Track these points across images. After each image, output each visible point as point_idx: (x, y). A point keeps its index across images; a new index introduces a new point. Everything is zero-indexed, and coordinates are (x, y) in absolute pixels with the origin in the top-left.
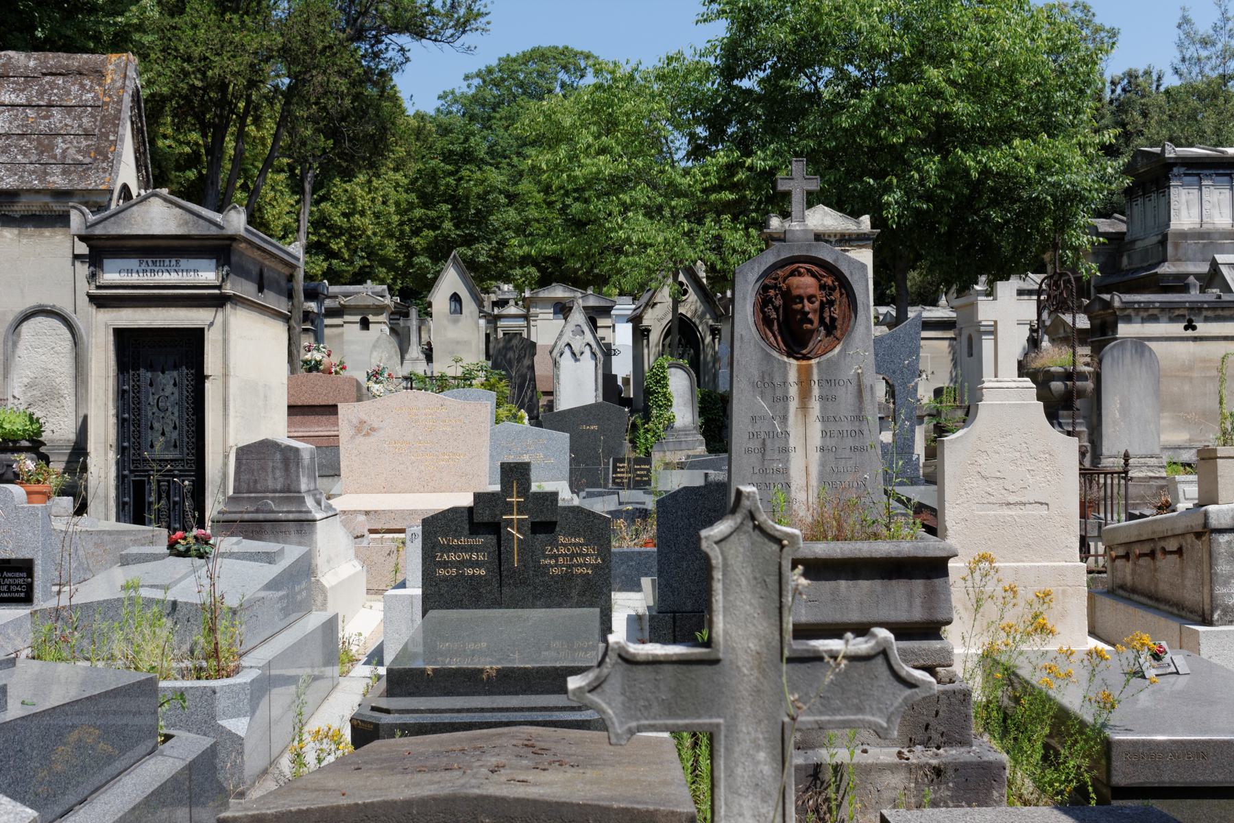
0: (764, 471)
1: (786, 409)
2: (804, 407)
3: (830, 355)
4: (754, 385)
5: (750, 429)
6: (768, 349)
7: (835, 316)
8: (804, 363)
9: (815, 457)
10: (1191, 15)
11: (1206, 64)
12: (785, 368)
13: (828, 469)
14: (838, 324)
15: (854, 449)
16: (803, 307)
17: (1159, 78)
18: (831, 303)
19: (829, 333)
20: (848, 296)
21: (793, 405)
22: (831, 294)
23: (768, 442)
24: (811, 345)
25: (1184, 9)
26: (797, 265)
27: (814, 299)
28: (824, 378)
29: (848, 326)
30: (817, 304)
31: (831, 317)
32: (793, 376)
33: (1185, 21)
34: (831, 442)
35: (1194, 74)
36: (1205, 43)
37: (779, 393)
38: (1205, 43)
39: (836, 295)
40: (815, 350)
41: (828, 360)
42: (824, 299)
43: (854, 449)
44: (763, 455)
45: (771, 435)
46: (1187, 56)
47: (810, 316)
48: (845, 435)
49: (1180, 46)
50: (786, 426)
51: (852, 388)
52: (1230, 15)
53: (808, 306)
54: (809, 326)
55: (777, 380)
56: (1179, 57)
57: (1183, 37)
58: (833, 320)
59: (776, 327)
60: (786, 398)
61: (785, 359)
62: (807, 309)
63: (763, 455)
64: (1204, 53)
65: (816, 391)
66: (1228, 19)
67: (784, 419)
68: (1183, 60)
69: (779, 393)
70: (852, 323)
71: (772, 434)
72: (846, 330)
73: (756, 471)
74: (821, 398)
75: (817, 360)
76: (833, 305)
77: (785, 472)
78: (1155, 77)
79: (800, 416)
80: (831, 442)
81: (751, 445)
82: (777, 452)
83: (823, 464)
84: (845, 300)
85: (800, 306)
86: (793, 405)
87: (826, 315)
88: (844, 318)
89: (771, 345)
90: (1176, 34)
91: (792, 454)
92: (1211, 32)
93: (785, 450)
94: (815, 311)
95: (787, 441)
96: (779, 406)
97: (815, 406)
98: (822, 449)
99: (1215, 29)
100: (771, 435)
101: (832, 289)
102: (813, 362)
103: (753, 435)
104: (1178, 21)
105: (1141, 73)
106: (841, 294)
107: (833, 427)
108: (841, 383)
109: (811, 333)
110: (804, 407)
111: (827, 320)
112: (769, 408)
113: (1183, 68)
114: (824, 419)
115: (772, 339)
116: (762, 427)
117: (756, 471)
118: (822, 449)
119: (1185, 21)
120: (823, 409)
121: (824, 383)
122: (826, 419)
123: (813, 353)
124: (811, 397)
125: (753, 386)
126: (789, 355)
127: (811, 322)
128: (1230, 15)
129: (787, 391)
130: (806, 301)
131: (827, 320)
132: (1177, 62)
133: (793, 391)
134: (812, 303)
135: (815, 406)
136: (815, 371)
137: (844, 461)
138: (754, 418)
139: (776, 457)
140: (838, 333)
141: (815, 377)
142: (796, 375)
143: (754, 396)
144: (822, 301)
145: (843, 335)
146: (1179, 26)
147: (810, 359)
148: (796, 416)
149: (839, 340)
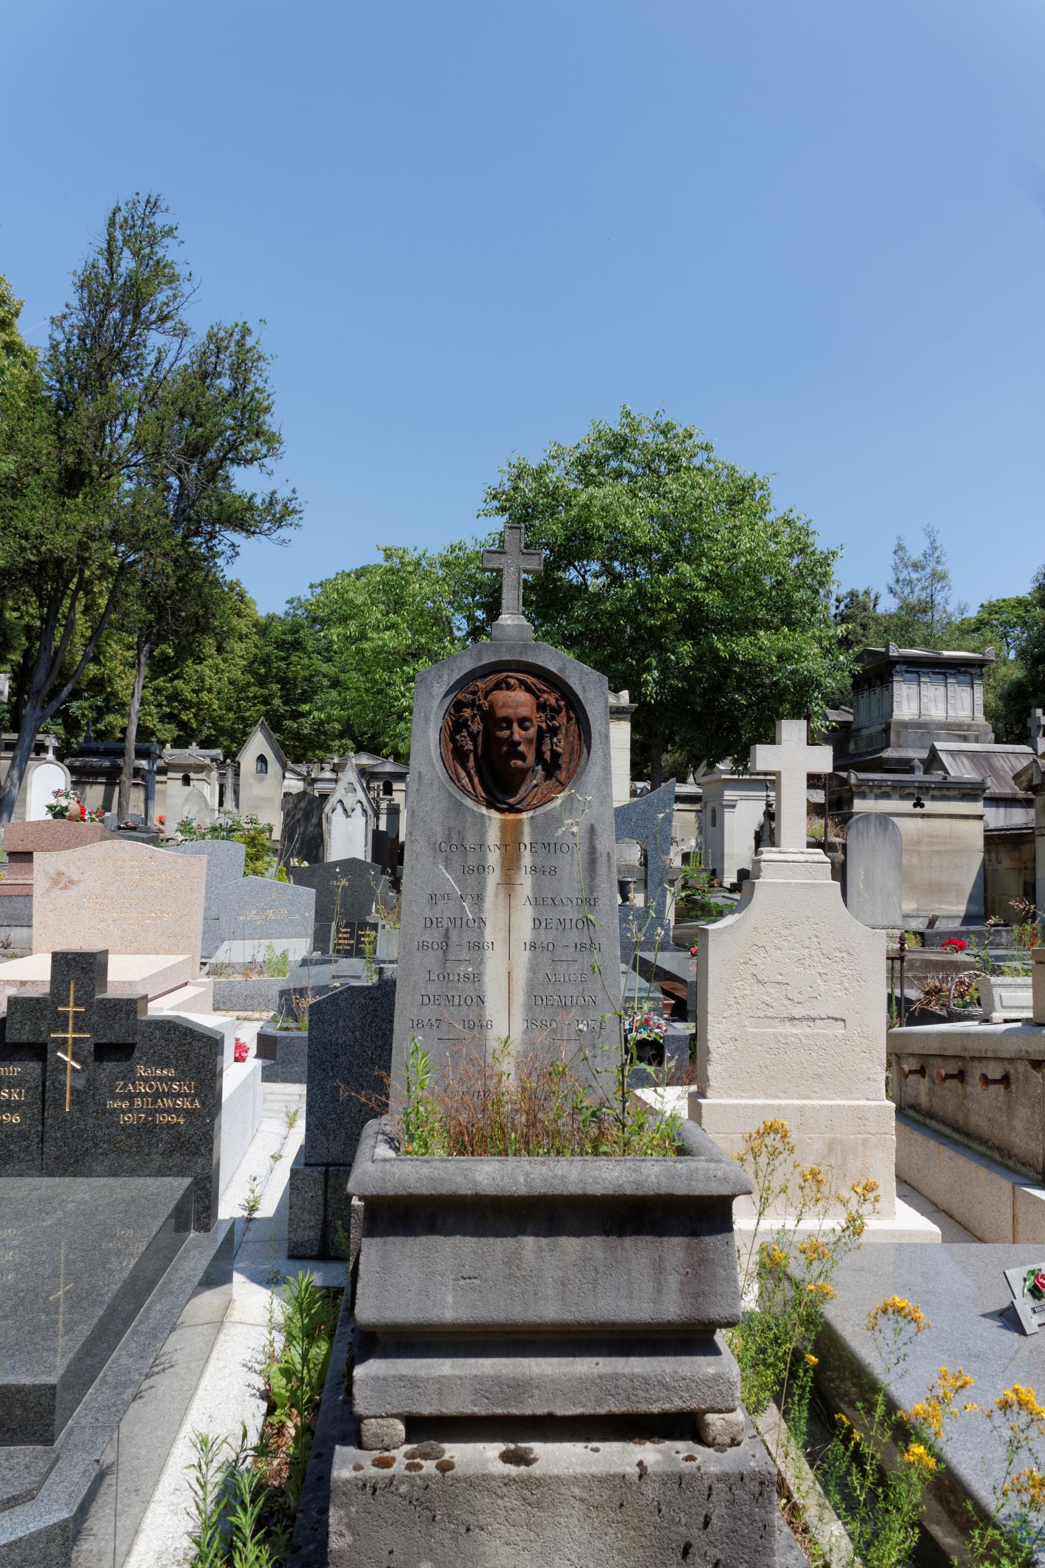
0: (445, 977)
1: (482, 885)
2: (508, 882)
3: (549, 806)
4: (436, 848)
5: (428, 914)
6: (459, 796)
7: (559, 750)
8: (511, 817)
9: (522, 958)
10: (906, 544)
11: (916, 585)
12: (483, 824)
13: (541, 977)
14: (563, 761)
15: (580, 947)
16: (512, 733)
17: (876, 598)
18: (554, 731)
19: (549, 775)
20: (578, 722)
21: (493, 879)
22: (553, 718)
23: (454, 934)
24: (522, 792)
25: (899, 538)
26: (505, 674)
27: (528, 724)
28: (540, 840)
29: (577, 765)
30: (532, 732)
31: (552, 750)
32: (493, 836)
33: (900, 548)
34: (546, 937)
35: (906, 593)
36: (916, 566)
37: (472, 860)
38: (916, 566)
39: (561, 720)
40: (528, 799)
41: (545, 814)
42: (544, 725)
43: (580, 947)
44: (445, 952)
45: (458, 922)
46: (901, 578)
47: (521, 748)
48: (568, 926)
49: (896, 569)
51: (580, 856)
52: (937, 544)
53: (518, 734)
54: (519, 763)
55: (471, 841)
56: (895, 578)
57: (898, 561)
58: (555, 755)
59: (471, 764)
60: (482, 869)
61: (484, 810)
62: (516, 737)
63: (445, 952)
64: (915, 576)
65: (527, 859)
66: (936, 548)
67: (479, 899)
68: (898, 581)
69: (472, 860)
70: (583, 761)
71: (460, 922)
72: (575, 771)
74: (534, 869)
75: (530, 813)
76: (556, 735)
77: (477, 978)
78: (873, 597)
79: (502, 896)
80: (546, 937)
81: (427, 937)
83: (533, 969)
84: (573, 727)
85: (508, 732)
86: (493, 879)
87: (546, 748)
88: (571, 754)
89: (463, 789)
90: (892, 559)
91: (488, 953)
92: (922, 558)
93: (478, 946)
94: (529, 742)
95: (482, 933)
96: (472, 880)
97: (525, 882)
98: (533, 946)
99: (925, 555)
100: (458, 922)
101: (556, 711)
102: (524, 816)
103: (431, 923)
104: (894, 548)
105: (861, 593)
106: (569, 719)
107: (550, 913)
108: (565, 848)
109: (523, 773)
110: (508, 882)
111: (548, 756)
112: (458, 882)
113: (897, 588)
114: (538, 902)
115: (466, 781)
116: (446, 911)
117: (434, 976)
118: (533, 946)
119: (900, 548)
120: (537, 886)
121: (539, 847)
122: (540, 901)
123: (525, 803)
124: (519, 868)
125: (434, 849)
126: (490, 805)
127: (522, 757)
128: (937, 544)
129: (483, 857)
130: (515, 726)
131: (548, 756)
132: (892, 582)
133: (494, 858)
134: (526, 729)
135: (525, 882)
136: (527, 829)
137: (565, 965)
138: (432, 897)
139: (465, 956)
140: (562, 775)
141: (527, 839)
143: (435, 864)
144: (540, 728)
145: (569, 778)
146: (895, 553)
147: (520, 811)
148: (496, 895)
149: (563, 785)
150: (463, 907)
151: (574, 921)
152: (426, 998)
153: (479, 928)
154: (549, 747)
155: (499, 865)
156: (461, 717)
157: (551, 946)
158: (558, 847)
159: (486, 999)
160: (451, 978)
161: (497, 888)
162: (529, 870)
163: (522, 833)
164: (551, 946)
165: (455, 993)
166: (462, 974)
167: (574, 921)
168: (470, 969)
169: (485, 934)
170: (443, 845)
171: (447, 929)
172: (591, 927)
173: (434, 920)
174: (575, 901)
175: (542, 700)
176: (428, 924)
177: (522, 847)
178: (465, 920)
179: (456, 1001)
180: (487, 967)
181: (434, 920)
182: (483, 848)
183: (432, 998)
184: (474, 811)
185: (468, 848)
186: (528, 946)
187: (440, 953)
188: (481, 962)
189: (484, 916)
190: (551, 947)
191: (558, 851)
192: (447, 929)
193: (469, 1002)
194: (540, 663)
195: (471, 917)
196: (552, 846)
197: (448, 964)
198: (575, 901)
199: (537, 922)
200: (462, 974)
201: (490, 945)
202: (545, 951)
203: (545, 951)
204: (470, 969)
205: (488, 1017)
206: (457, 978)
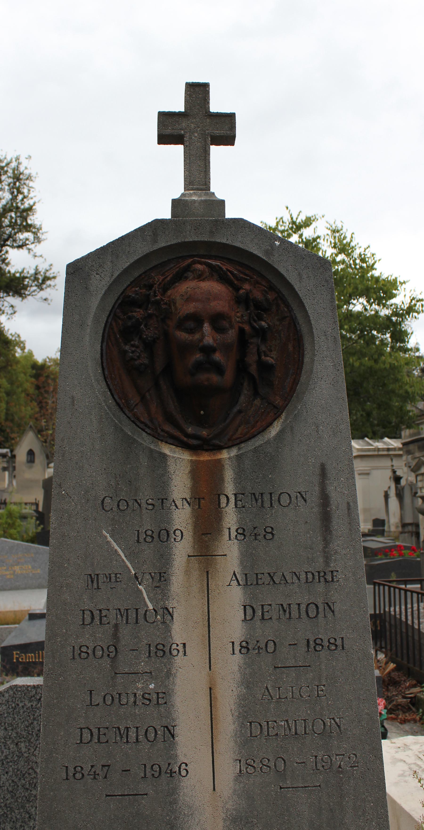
3: (259, 441)
6: (129, 429)
7: (270, 360)
8: (205, 457)
16: (203, 336)
30: (232, 335)
41: (256, 450)
42: (247, 328)
44: (114, 660)
45: (132, 615)
47: (217, 357)
48: (295, 613)
50: (165, 595)
63: (114, 660)
73: (97, 699)
75: (234, 452)
79: (195, 574)
82: (144, 656)
87: (252, 359)
91: (179, 660)
95: (168, 629)
100: (132, 615)
102: (225, 455)
108: (285, 500)
111: (253, 369)
115: (140, 410)
117: (97, 699)
139: (142, 666)
142: (188, 483)
147: (220, 448)
148: (187, 572)
150: (140, 591)
151: (303, 607)
152: (85, 731)
153: (164, 622)
154: (256, 358)
155: (190, 527)
156: (130, 318)
157: (271, 644)
158: (275, 498)
159: (177, 731)
160: (124, 701)
161: (188, 562)
162: (234, 534)
163: (222, 480)
164: (271, 644)
165: (130, 724)
166: (140, 693)
167: (303, 607)
168: (152, 686)
169: (173, 632)
170: (108, 500)
171: (116, 626)
172: (330, 615)
173: (96, 613)
174: (303, 576)
175: (241, 292)
176: (88, 619)
177: (223, 500)
178: (141, 612)
179: (132, 734)
180: (178, 681)
181: (96, 613)
182: (167, 504)
183: (95, 731)
184: (151, 451)
185: (144, 505)
186: (237, 648)
187: (106, 662)
188: (169, 674)
189: (170, 606)
190: (271, 649)
191: (276, 505)
192: (116, 626)
193: (151, 736)
194: (238, 244)
195: (151, 607)
196: (266, 498)
197: (120, 679)
198: (303, 576)
199: (249, 611)
200: (140, 693)
201: (180, 648)
202: (263, 652)
203: (263, 652)
204: (152, 686)
205: (182, 759)
206: (132, 699)
